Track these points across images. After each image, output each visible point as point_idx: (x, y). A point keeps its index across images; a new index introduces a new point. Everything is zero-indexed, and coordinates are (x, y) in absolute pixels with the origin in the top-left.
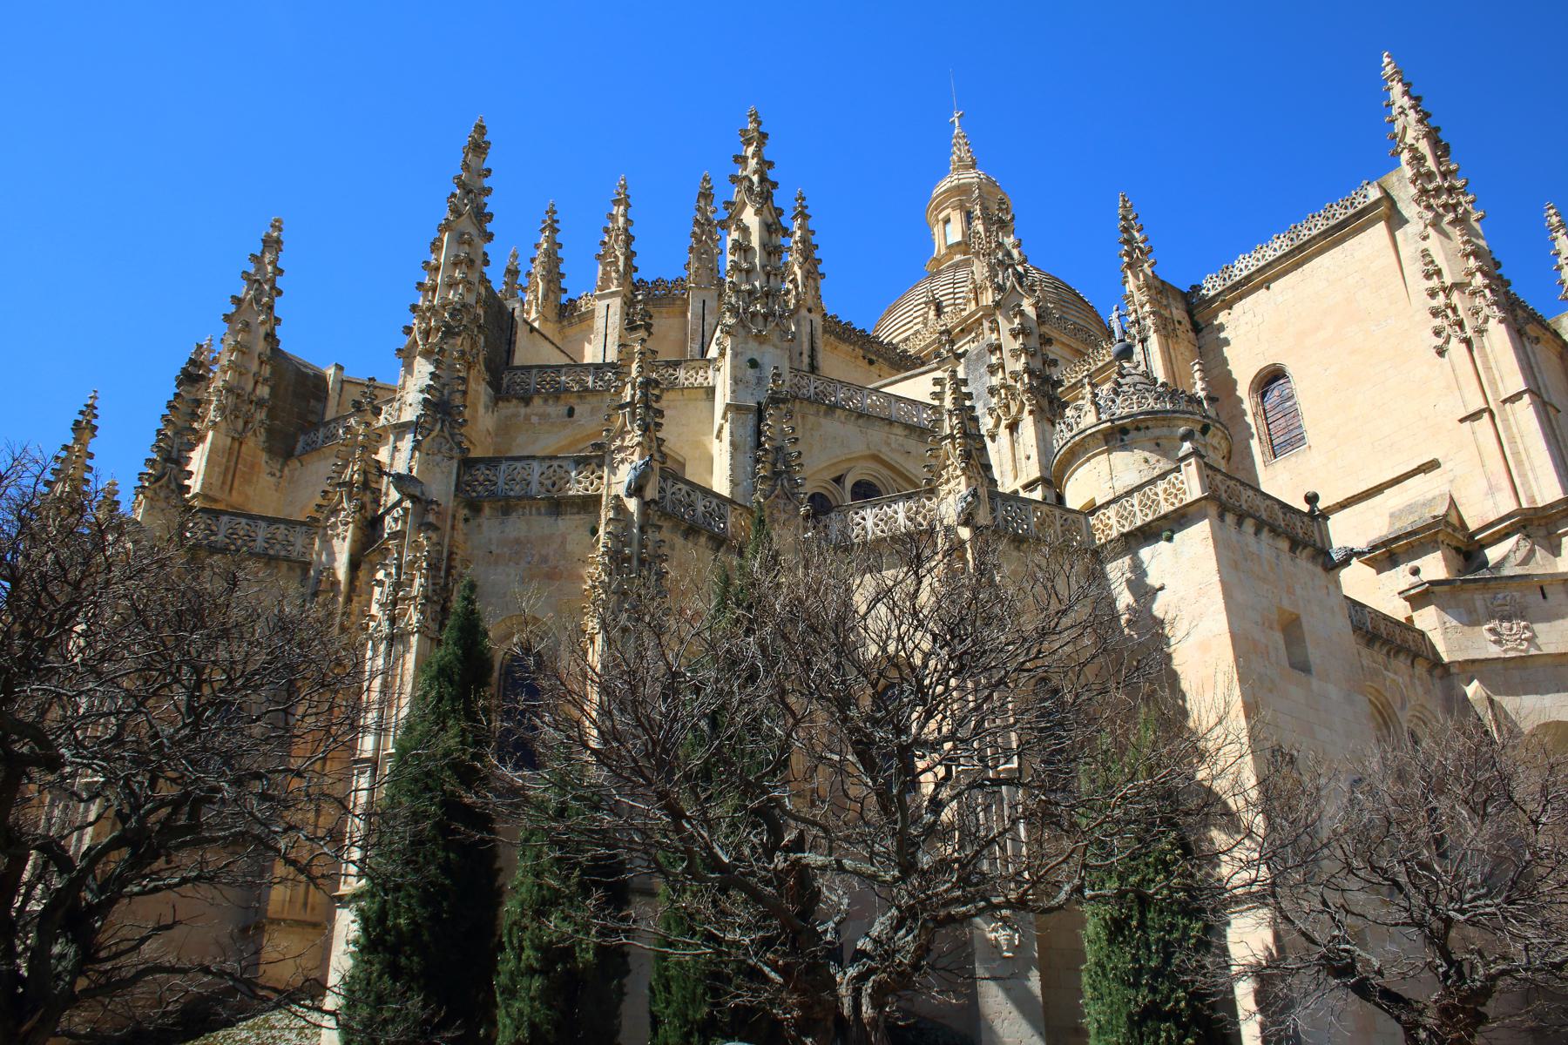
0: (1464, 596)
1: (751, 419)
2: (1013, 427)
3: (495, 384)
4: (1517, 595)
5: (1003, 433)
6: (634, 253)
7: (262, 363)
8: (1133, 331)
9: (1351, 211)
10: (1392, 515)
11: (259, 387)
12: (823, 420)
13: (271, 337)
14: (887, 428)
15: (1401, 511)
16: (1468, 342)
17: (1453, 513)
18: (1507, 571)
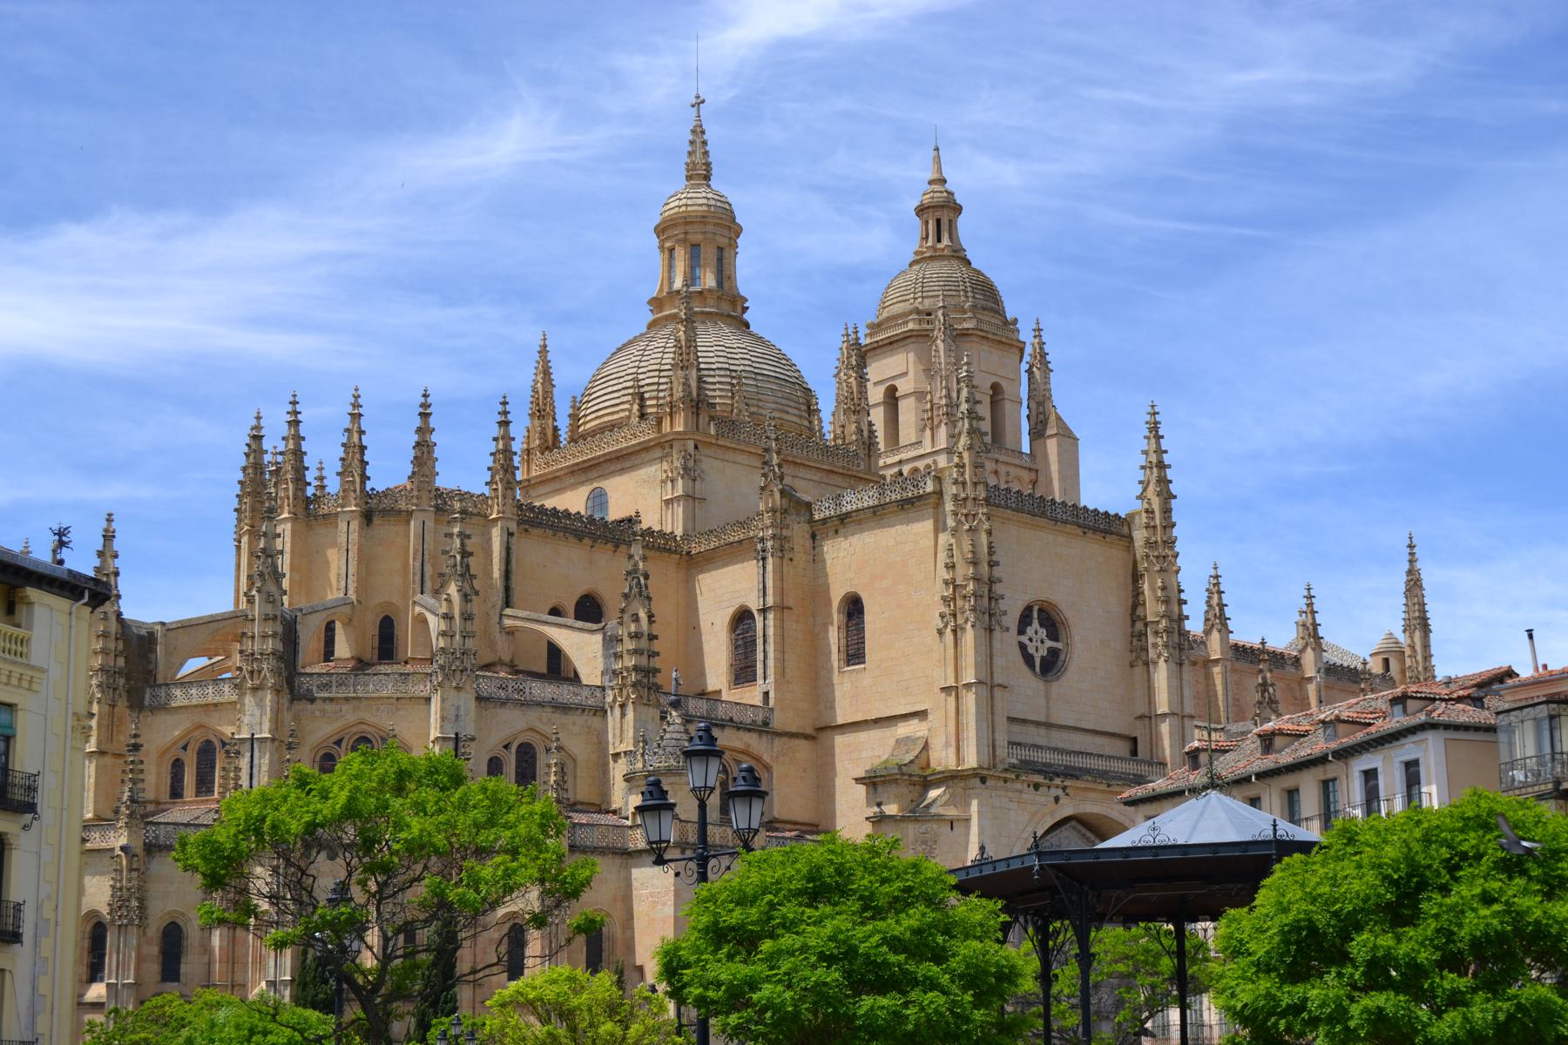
0: (902, 825)
1: (451, 745)
2: (622, 706)
3: (292, 691)
4: (935, 826)
5: (617, 711)
6: (367, 463)
7: (117, 639)
8: (759, 547)
9: (916, 494)
10: (897, 741)
11: (118, 659)
12: (499, 711)
13: (119, 614)
14: (541, 709)
15: (902, 739)
16: (954, 631)
17: (924, 756)
18: (933, 810)
